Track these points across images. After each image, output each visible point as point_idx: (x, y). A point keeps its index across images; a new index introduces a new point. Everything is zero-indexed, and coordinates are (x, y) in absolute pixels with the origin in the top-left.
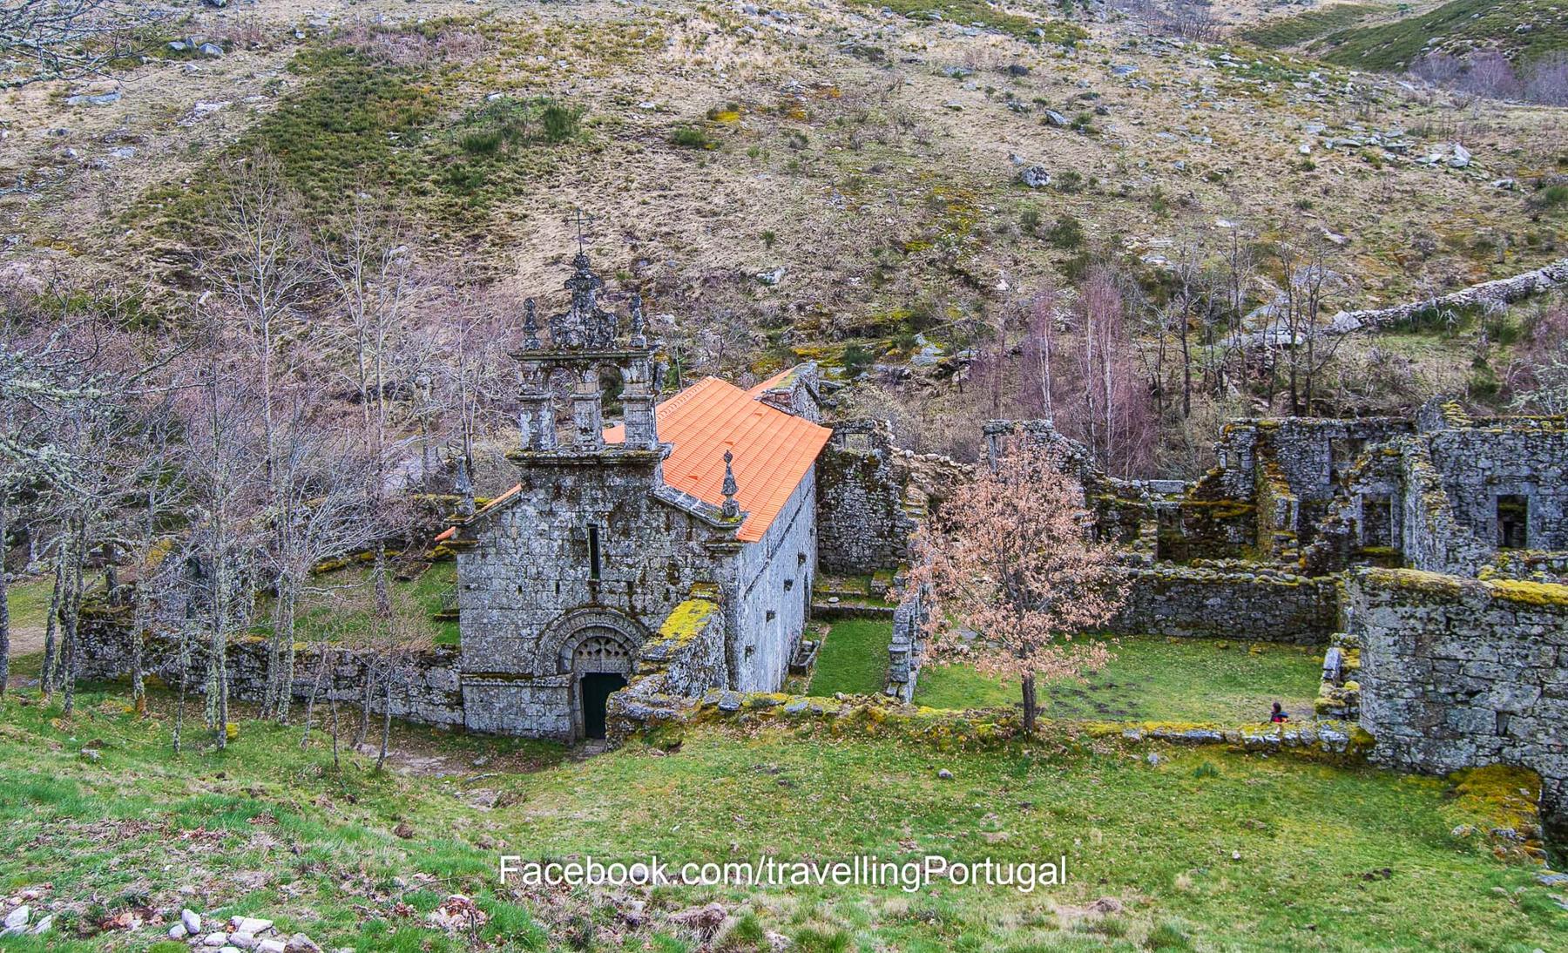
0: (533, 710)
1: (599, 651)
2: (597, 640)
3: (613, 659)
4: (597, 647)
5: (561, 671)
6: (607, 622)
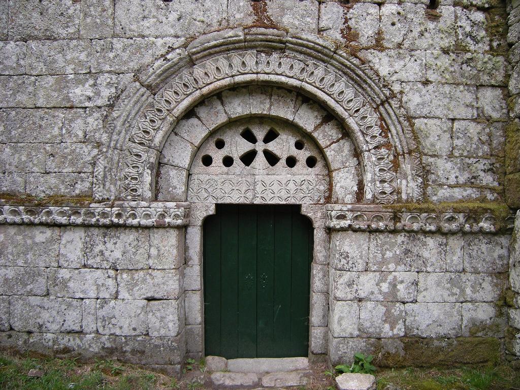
0: (89, 283)
1: (248, 158)
2: (245, 126)
4: (245, 146)
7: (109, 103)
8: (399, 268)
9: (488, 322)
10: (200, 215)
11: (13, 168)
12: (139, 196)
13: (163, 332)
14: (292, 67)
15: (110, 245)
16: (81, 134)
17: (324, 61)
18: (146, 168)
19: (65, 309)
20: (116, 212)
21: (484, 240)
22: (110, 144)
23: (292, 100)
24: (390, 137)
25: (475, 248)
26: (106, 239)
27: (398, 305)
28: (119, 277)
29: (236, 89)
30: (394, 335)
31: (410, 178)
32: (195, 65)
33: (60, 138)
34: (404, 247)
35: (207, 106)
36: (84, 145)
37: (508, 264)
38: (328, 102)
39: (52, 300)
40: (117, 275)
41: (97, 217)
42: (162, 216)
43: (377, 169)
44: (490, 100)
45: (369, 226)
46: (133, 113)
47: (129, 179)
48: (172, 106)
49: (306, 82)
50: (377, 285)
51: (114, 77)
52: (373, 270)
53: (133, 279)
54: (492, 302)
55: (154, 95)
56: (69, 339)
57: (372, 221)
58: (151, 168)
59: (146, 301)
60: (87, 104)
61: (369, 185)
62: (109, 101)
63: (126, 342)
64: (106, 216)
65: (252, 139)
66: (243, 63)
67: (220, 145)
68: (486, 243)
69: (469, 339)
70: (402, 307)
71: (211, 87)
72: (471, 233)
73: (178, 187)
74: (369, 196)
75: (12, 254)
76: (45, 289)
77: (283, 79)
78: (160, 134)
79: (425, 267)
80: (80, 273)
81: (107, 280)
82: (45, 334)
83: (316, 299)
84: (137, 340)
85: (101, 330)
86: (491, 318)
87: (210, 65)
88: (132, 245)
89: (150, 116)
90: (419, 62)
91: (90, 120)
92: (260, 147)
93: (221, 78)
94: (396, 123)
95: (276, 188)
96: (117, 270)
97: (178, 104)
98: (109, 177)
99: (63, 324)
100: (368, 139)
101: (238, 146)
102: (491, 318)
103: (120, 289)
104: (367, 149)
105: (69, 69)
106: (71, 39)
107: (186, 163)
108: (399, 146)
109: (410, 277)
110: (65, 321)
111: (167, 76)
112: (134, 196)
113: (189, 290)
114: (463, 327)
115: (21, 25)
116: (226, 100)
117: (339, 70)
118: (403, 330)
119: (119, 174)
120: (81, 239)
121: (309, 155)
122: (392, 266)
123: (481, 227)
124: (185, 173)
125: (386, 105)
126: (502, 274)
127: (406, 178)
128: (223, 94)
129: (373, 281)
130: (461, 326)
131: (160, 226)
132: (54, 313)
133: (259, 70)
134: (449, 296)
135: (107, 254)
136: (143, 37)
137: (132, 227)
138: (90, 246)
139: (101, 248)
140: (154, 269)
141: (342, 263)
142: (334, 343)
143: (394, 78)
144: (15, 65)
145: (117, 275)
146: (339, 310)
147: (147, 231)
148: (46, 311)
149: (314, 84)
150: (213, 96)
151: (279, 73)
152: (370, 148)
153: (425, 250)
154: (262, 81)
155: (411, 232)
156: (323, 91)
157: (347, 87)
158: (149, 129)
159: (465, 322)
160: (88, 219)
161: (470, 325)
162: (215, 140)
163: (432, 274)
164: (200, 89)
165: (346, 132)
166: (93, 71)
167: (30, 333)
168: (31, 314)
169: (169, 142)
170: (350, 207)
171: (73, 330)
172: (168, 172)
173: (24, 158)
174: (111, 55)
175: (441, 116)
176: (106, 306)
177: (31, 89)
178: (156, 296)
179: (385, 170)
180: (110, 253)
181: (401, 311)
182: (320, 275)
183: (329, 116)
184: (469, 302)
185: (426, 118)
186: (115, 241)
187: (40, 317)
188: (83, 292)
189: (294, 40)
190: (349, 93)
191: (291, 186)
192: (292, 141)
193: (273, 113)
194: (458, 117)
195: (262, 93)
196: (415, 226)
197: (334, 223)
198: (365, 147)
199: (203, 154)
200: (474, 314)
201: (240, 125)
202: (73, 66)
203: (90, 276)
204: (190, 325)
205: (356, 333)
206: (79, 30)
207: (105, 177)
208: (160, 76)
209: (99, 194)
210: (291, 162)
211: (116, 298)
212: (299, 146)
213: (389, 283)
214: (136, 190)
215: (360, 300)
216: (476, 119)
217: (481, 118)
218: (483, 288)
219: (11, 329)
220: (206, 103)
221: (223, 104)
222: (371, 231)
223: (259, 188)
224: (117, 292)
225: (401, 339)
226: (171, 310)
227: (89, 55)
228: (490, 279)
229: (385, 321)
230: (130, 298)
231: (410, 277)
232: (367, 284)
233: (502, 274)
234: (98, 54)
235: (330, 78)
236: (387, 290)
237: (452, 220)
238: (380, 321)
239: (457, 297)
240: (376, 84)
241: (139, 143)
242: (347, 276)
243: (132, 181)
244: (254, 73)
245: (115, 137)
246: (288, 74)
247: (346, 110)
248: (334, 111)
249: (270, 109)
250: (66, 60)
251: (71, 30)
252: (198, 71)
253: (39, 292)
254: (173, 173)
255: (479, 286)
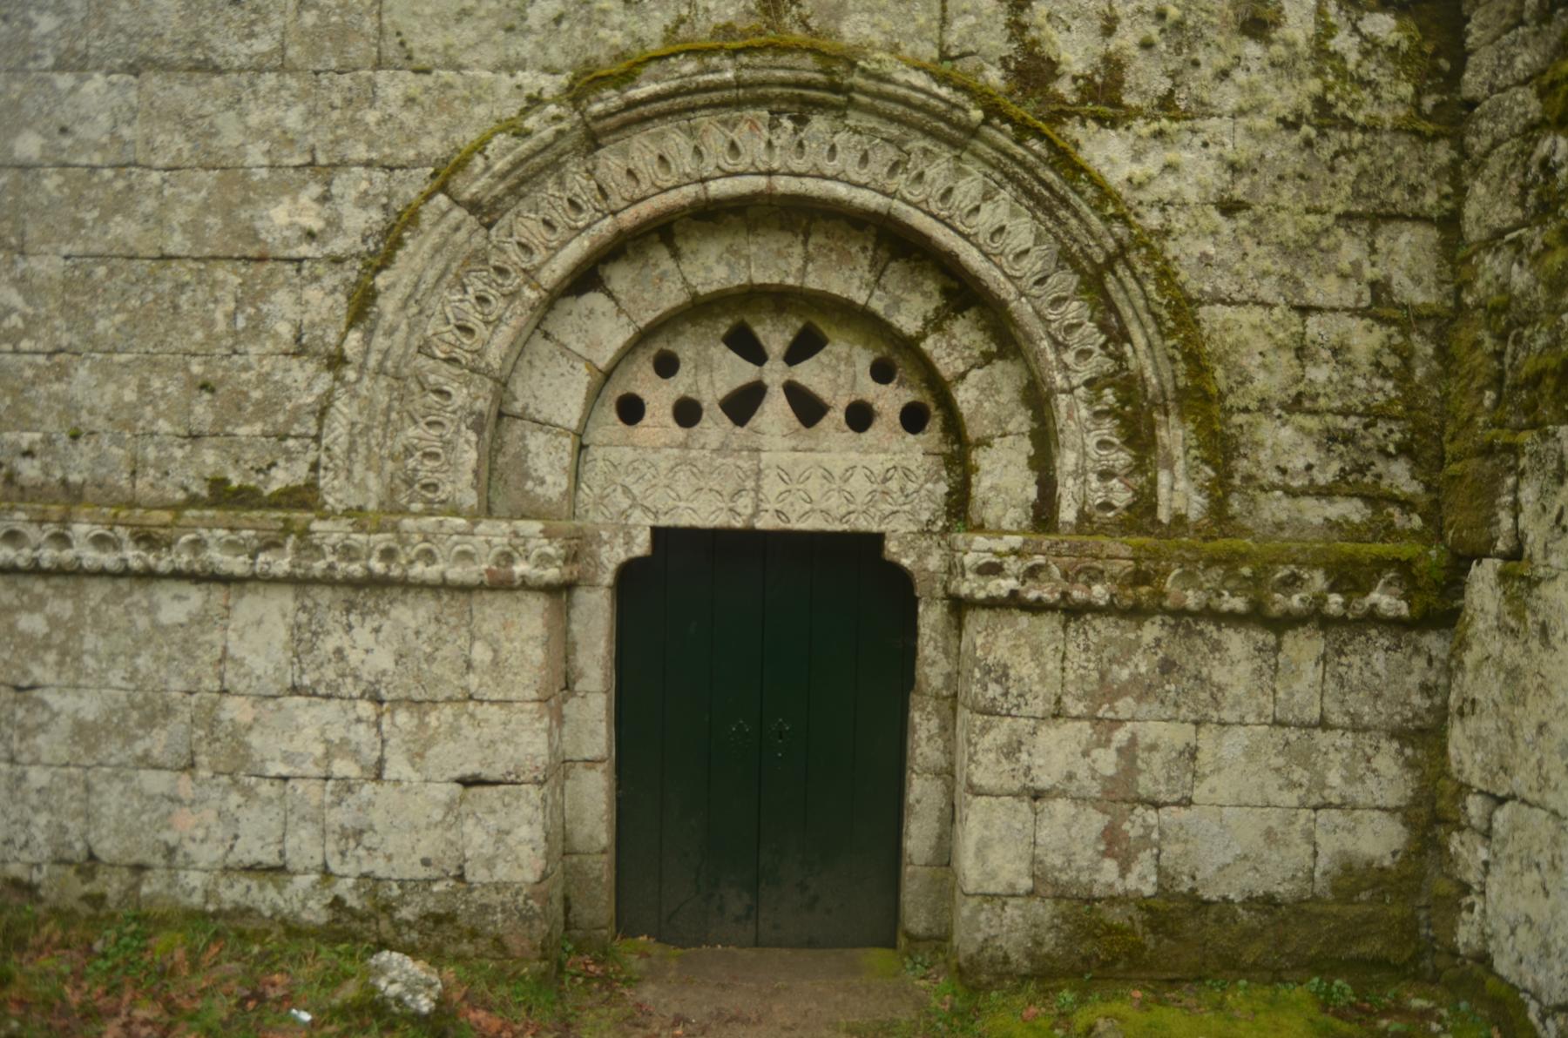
1: (742, 405)
2: (735, 316)
3: (833, 441)
4: (734, 372)
5: (499, 484)
6: (838, 164)
7: (363, 248)
8: (1145, 707)
9: (1386, 863)
10: (613, 555)
11: (100, 423)
12: (443, 502)
13: (502, 872)
14: (864, 160)
15: (363, 635)
16: (285, 330)
17: (952, 143)
18: (463, 427)
19: (239, 806)
20: (382, 546)
21: (1381, 640)
22: (365, 360)
23: (864, 249)
24: (1130, 354)
25: (1356, 660)
26: (353, 618)
27: (1140, 810)
28: (386, 721)
29: (712, 216)
30: (1127, 892)
31: (1180, 466)
32: (599, 147)
33: (230, 341)
34: (1161, 654)
35: (634, 261)
36: (295, 363)
37: (1445, 705)
38: (963, 257)
39: (204, 781)
40: (380, 715)
41: (331, 558)
42: (507, 558)
43: (1092, 441)
44: (1406, 258)
45: (1065, 595)
46: (431, 276)
47: (418, 454)
48: (537, 259)
49: (904, 200)
50: (1085, 754)
51: (379, 175)
52: (1074, 713)
53: (423, 725)
54: (1397, 809)
55: (489, 226)
56: (249, 888)
57: (1074, 581)
58: (478, 427)
59: (458, 788)
60: (305, 250)
61: (1070, 482)
62: (364, 241)
63: (403, 895)
64: (353, 555)
65: (753, 351)
66: (733, 147)
67: (667, 366)
68: (1387, 649)
69: (1335, 909)
70: (1151, 816)
71: (644, 210)
72: (1342, 621)
73: (549, 479)
74: (1068, 514)
75: (94, 654)
76: (184, 751)
77: (841, 191)
78: (505, 333)
79: (1216, 710)
80: (280, 708)
81: (353, 728)
82: (182, 873)
83: (921, 791)
84: (432, 893)
85: (335, 865)
86: (1394, 854)
87: (641, 149)
88: (424, 636)
89: (476, 285)
90: (1213, 150)
91: (312, 293)
92: (774, 374)
93: (670, 184)
94: (1146, 317)
95: (815, 486)
96: (381, 702)
97: (553, 256)
98: (362, 450)
99: (232, 847)
100: (1069, 357)
101: (715, 372)
102: (1394, 854)
103: (387, 754)
104: (1066, 386)
105: (256, 154)
106: (260, 70)
107: (571, 414)
108: (1154, 381)
109: (1176, 735)
110: (236, 837)
111: (524, 179)
112: (431, 502)
113: (575, 757)
114: (1317, 875)
115: (121, 30)
116: (685, 248)
117: (993, 167)
118: (1154, 878)
119: (389, 443)
120: (284, 616)
121: (909, 399)
122: (1125, 706)
123: (1374, 606)
124: (568, 443)
125: (1120, 269)
126: (1424, 737)
127: (1169, 464)
128: (677, 228)
129: (1074, 745)
130: (1312, 871)
131: (500, 585)
132: (210, 816)
133: (775, 165)
134: (1280, 788)
135: (354, 657)
136: (459, 68)
137: (423, 586)
138: (308, 635)
139: (338, 643)
140: (481, 701)
141: (990, 694)
142: (965, 912)
143: (1146, 196)
144: (105, 139)
145: (380, 715)
146: (976, 822)
147: (462, 597)
148: (186, 810)
149: (924, 206)
150: (647, 234)
151: (829, 172)
152: (1075, 382)
153: (1215, 663)
154: (784, 196)
155: (1180, 613)
156: (948, 225)
157: (1014, 214)
158: (474, 320)
159: (1323, 863)
160: (304, 562)
161: (1337, 871)
162: (654, 352)
163: (1235, 728)
164: (614, 213)
165: (1005, 339)
166: (322, 159)
167: (139, 869)
168: (145, 818)
169: (527, 357)
170: (1016, 541)
171: (260, 863)
172: (523, 438)
173: (130, 396)
174: (371, 117)
175: (1270, 300)
176: (351, 800)
177: (149, 204)
178: (487, 773)
179: (1112, 444)
180: (364, 656)
181: (1148, 828)
182: (934, 724)
183: (963, 293)
184: (1338, 807)
185: (1229, 305)
186: (376, 624)
187: (169, 827)
188: (288, 758)
189: (871, 85)
190: (1022, 231)
191: (859, 484)
192: (863, 360)
193: (813, 282)
194: (1319, 300)
195: (782, 228)
196: (1192, 599)
197: (968, 586)
198: (1059, 380)
199: (619, 392)
200: (1349, 843)
201: (718, 316)
202: (266, 146)
203: (312, 721)
204: (576, 853)
205: (1025, 883)
206: (283, 48)
207: (352, 448)
208: (503, 176)
209: (335, 491)
210: (860, 416)
211: (378, 777)
212: (882, 372)
213: (1119, 750)
214: (433, 487)
215: (1038, 795)
216: (1369, 307)
217: (1379, 304)
218: (1374, 771)
219: (92, 857)
220: (630, 252)
221: (676, 255)
222: (1073, 611)
223: (772, 486)
224: (381, 763)
225: (1143, 904)
226: (527, 810)
227: (312, 113)
228: (1396, 745)
229: (1105, 854)
230: (416, 777)
231: (1176, 735)
232: (1056, 752)
233: (1424, 737)
234: (336, 115)
235: (969, 188)
236: (1110, 771)
237: (1293, 583)
238: (1090, 852)
239: (1302, 792)
240: (1095, 209)
241: (445, 360)
242: (1001, 732)
243: (426, 462)
244: (760, 173)
245: (380, 341)
246: (855, 178)
247: (1010, 278)
248: (976, 279)
249: (803, 271)
250: (247, 128)
251: (263, 45)
252: (610, 162)
253: (167, 758)
254: (536, 441)
255: (1363, 765)
